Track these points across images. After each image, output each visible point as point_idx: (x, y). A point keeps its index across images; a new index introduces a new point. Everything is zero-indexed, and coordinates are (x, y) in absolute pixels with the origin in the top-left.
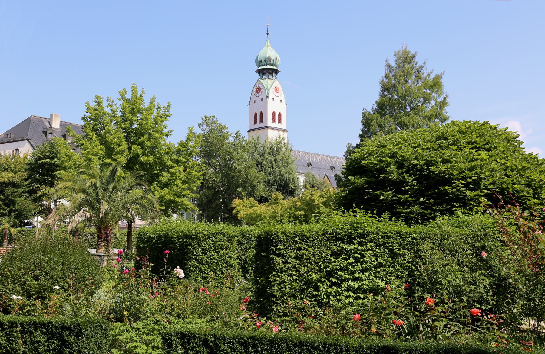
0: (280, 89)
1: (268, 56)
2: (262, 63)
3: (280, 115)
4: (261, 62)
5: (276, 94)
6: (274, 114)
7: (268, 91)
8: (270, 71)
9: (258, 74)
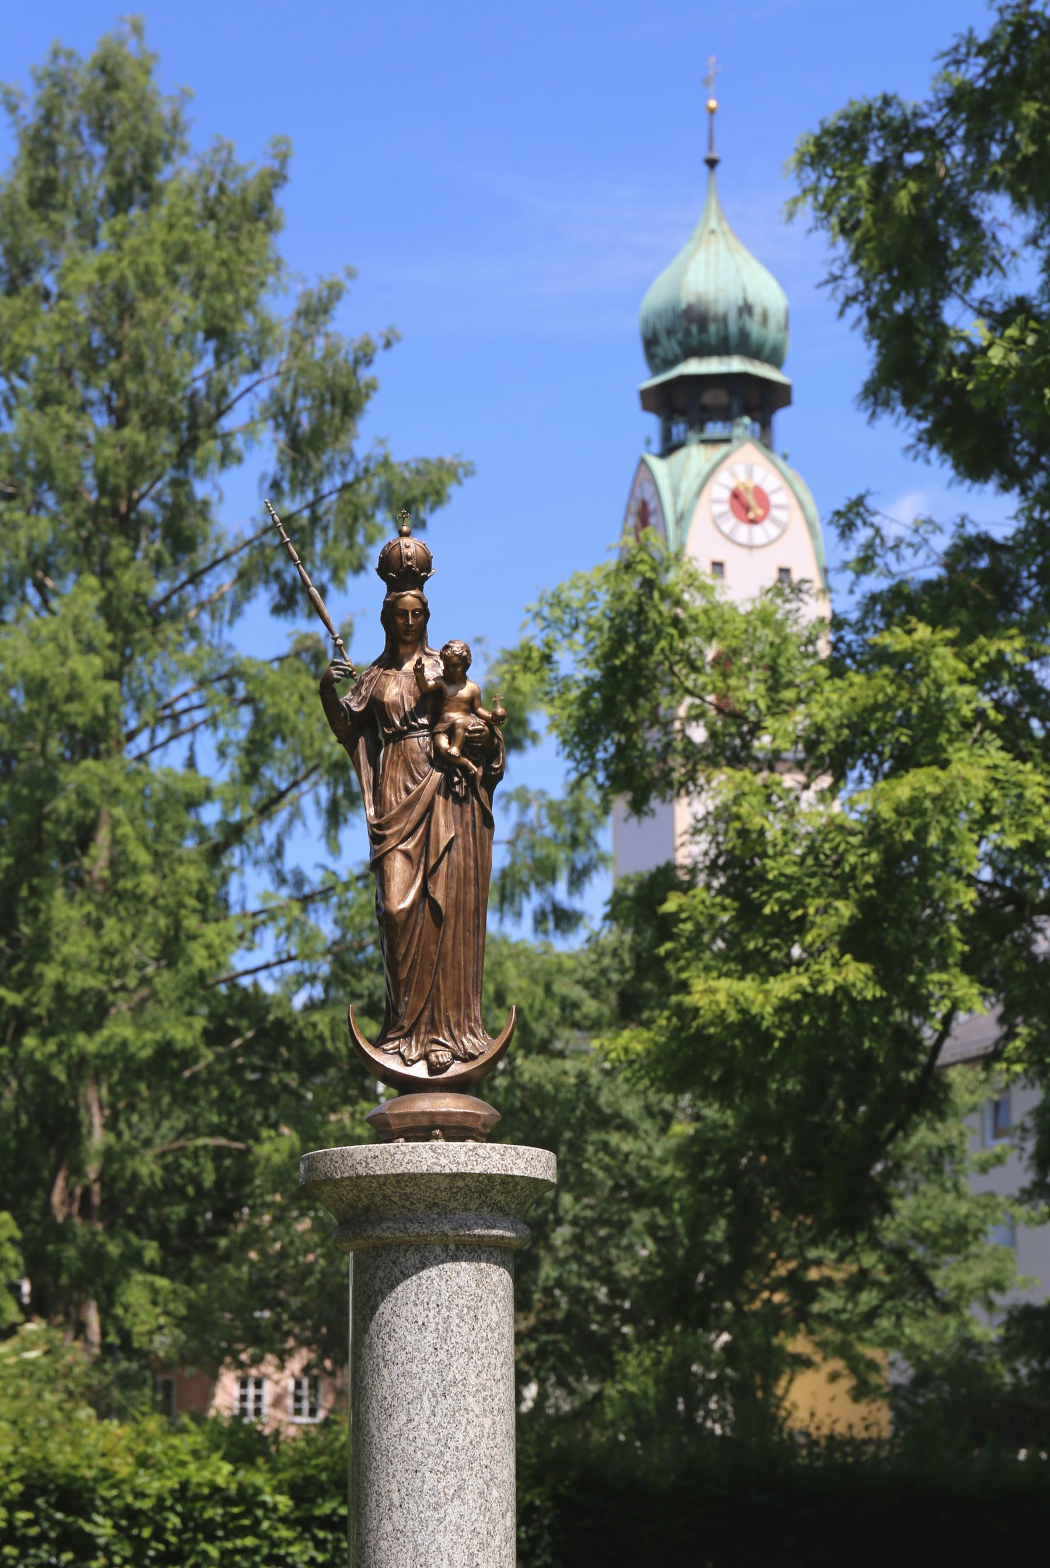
0: (774, 499)
1: (687, 297)
5: (743, 532)
7: (682, 519)
8: (711, 397)
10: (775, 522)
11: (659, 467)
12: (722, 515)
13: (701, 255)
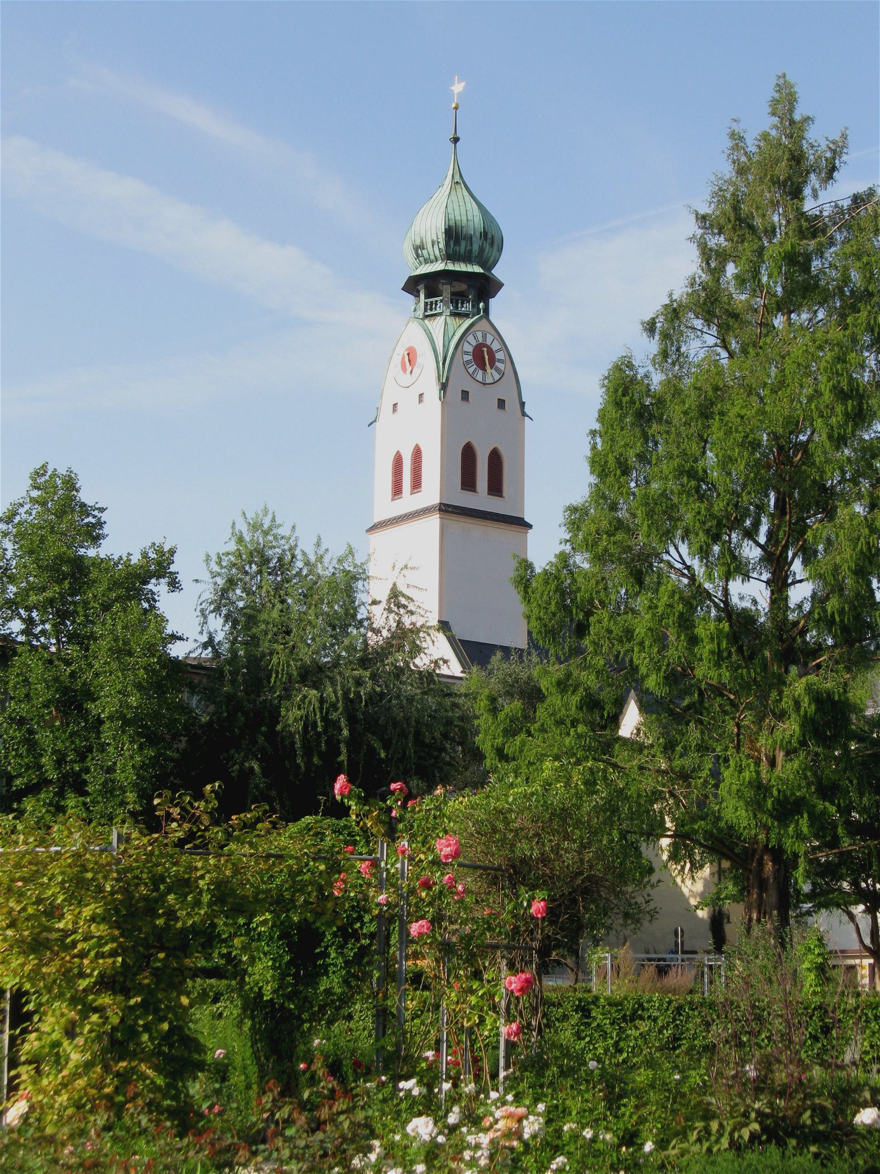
2: (425, 252)
3: (495, 459)
4: (422, 247)
6: (468, 454)
10: (498, 370)
12: (468, 362)
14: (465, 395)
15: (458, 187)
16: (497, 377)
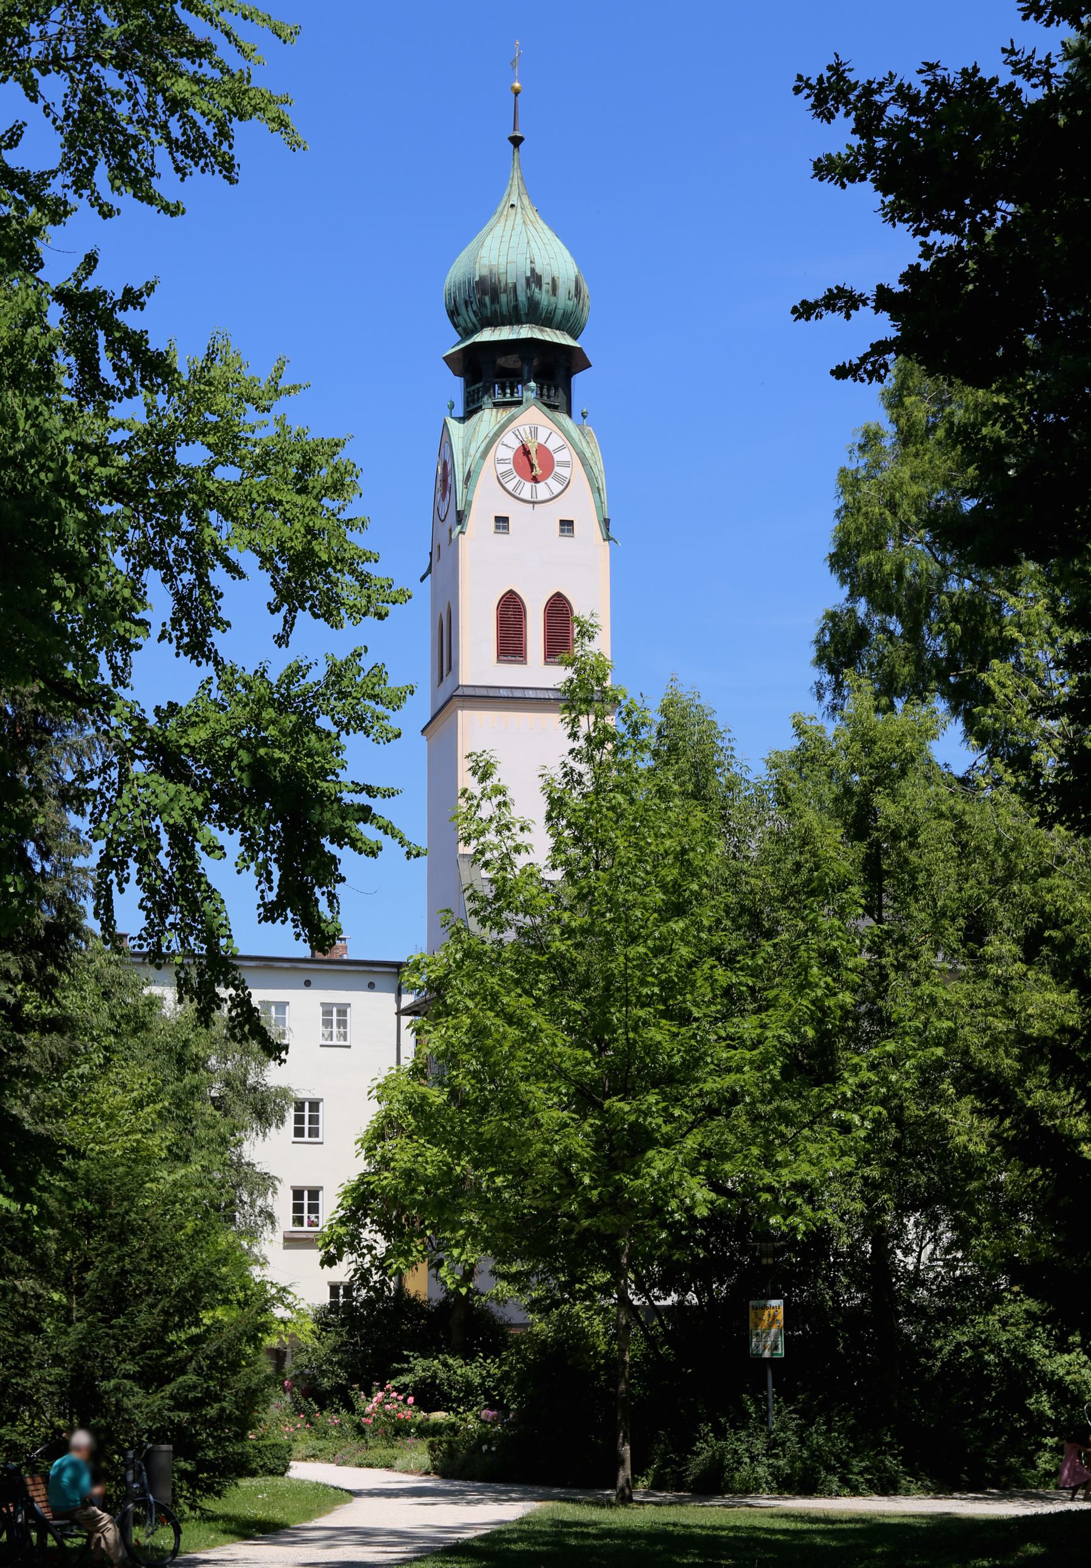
0: (557, 457)
1: (481, 270)
5: (526, 490)
8: (503, 361)
9: (458, 383)
10: (559, 478)
11: (456, 429)
12: (505, 474)
13: (498, 230)
14: (502, 522)
15: (512, 211)
16: (557, 488)
